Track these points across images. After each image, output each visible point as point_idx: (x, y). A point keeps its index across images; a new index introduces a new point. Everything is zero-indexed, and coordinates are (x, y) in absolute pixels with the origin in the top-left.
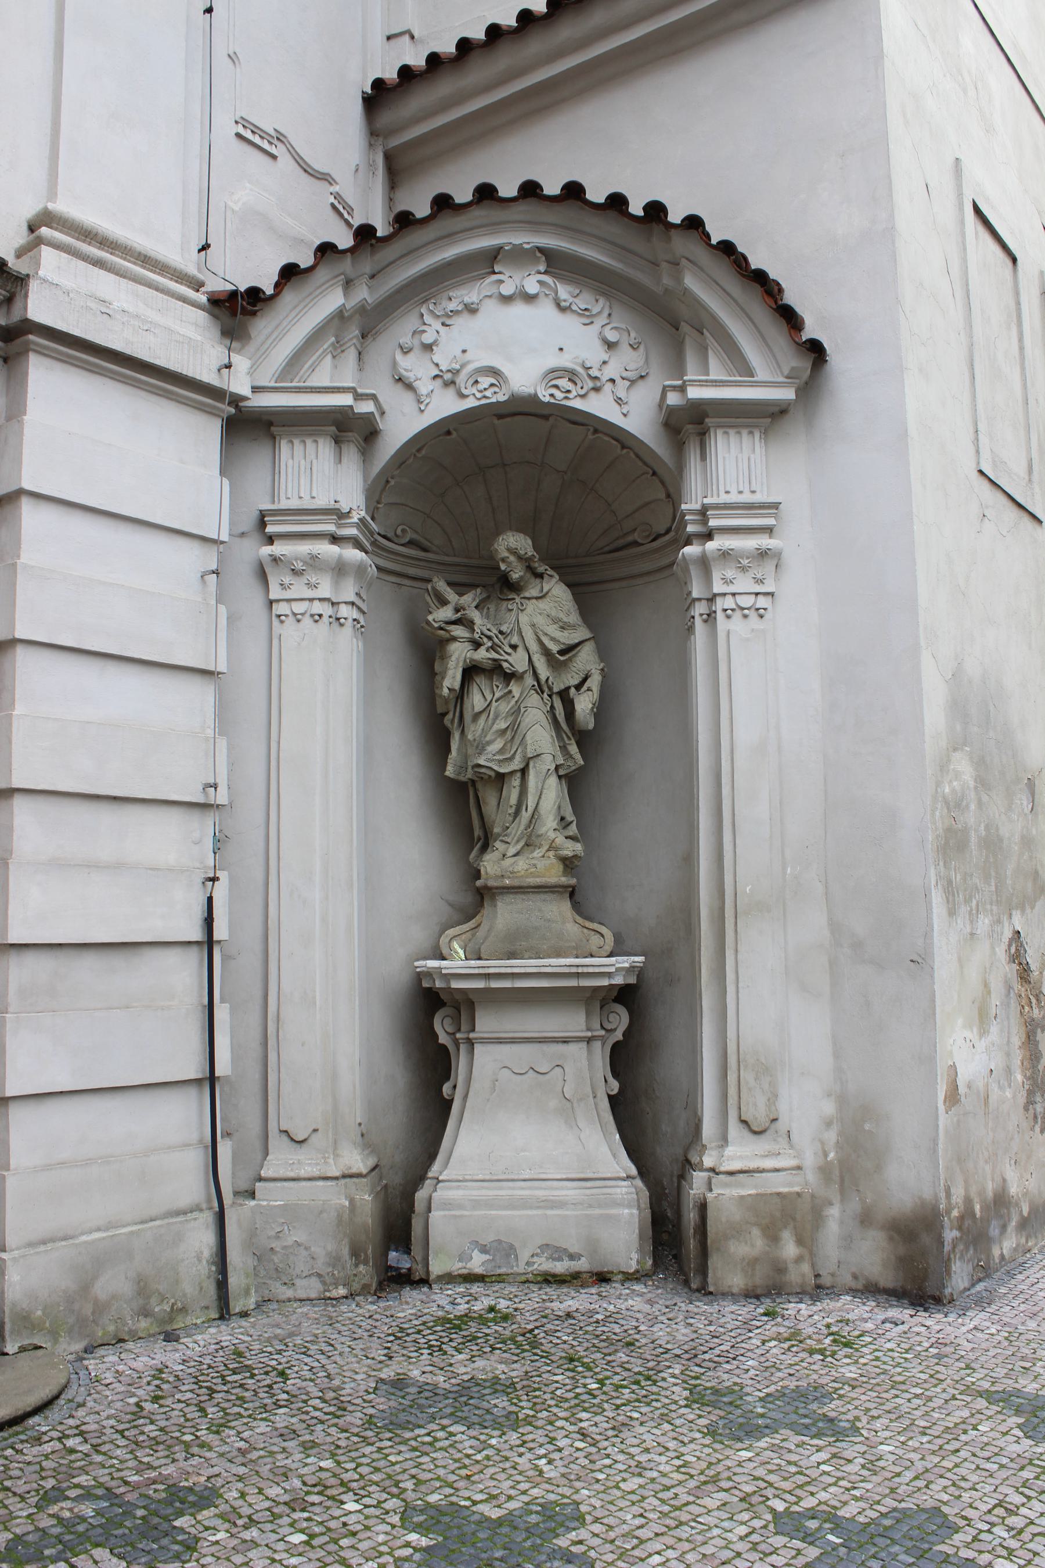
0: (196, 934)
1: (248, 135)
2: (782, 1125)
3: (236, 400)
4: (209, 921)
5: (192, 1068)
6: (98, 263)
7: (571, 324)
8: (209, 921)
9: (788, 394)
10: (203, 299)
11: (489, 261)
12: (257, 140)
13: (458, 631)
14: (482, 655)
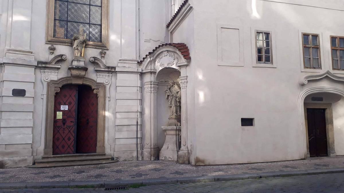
0: (136, 124)
1: (146, 41)
2: (187, 145)
3: (140, 72)
4: (137, 123)
5: (136, 137)
6: (124, 63)
7: (170, 57)
8: (137, 123)
9: (186, 64)
10: (137, 62)
11: (162, 52)
12: (147, 41)
13: (167, 91)
14: (169, 94)
